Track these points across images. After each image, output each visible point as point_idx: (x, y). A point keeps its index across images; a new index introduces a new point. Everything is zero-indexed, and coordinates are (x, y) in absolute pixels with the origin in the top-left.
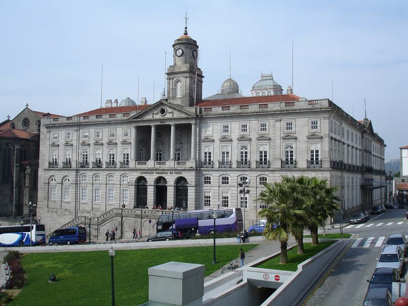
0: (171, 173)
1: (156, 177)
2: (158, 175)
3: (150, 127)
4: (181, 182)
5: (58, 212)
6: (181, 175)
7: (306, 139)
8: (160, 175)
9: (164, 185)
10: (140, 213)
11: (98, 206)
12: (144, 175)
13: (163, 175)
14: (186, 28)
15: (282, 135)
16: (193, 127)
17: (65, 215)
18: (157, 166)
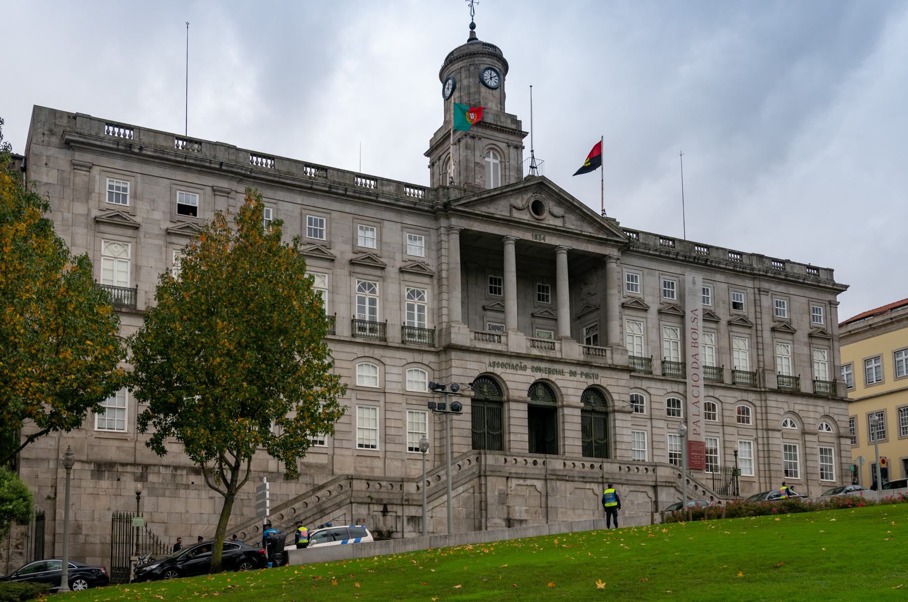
0: (573, 374)
1: (532, 381)
2: (539, 376)
3: (500, 241)
4: (595, 394)
5: (152, 478)
6: (597, 382)
7: (806, 339)
8: (545, 376)
9: (551, 404)
10: (562, 467)
11: (323, 460)
12: (498, 371)
13: (553, 377)
14: (473, 26)
15: (773, 324)
16: (612, 266)
17: (187, 487)
18: (535, 352)
